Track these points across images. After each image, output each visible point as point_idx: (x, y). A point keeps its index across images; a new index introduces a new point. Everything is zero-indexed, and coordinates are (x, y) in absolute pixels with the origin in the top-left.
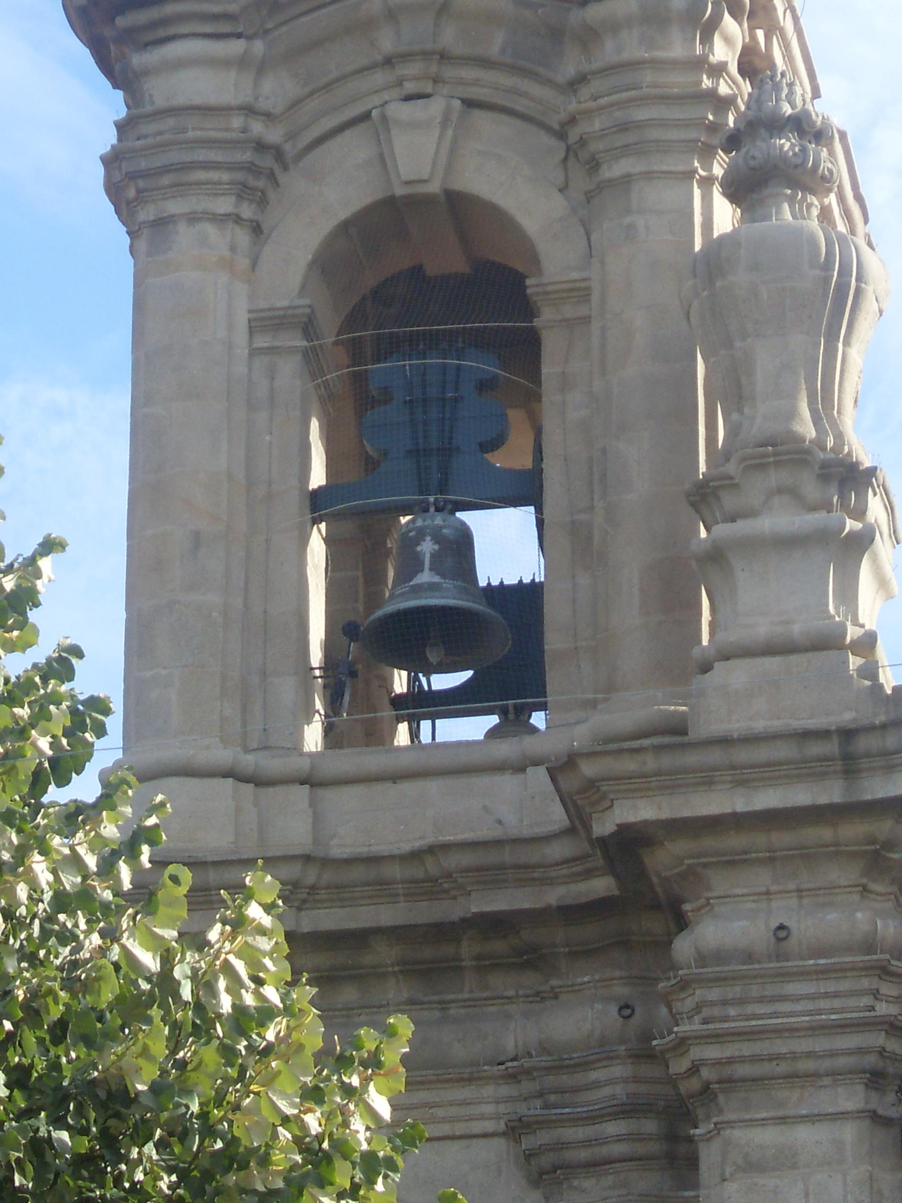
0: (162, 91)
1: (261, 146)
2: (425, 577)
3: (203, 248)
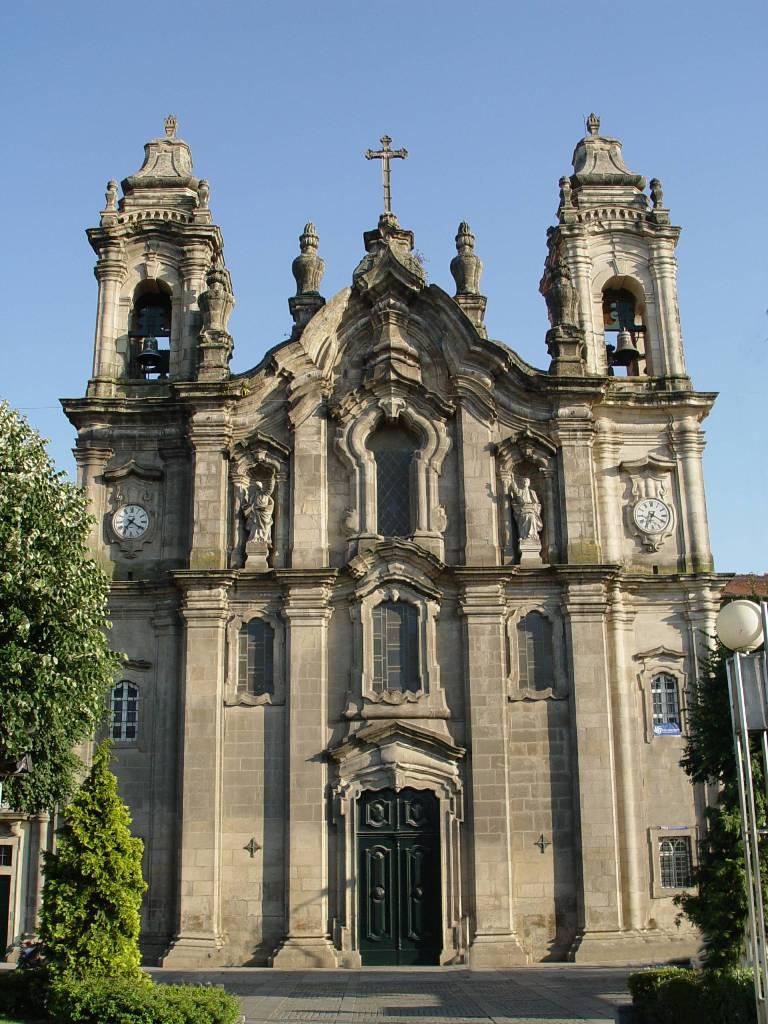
2: (149, 349)
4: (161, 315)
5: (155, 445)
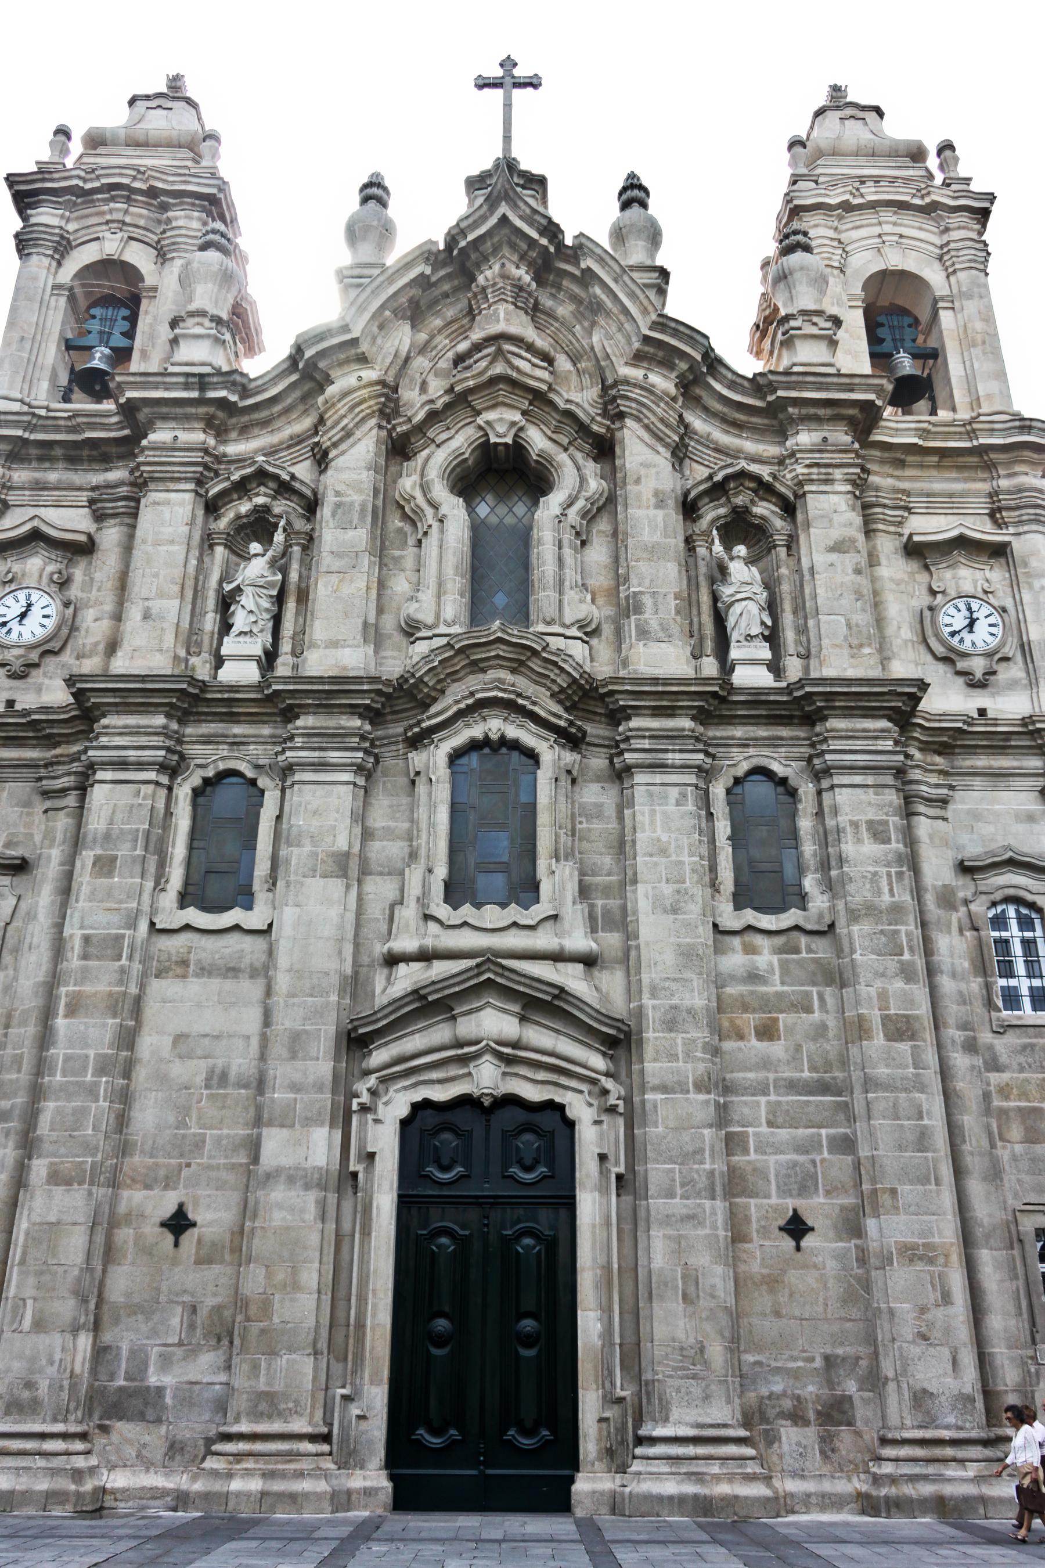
0: (33, 220)
1: (62, 237)
3: (40, 263)
4: (124, 318)
5: (84, 497)
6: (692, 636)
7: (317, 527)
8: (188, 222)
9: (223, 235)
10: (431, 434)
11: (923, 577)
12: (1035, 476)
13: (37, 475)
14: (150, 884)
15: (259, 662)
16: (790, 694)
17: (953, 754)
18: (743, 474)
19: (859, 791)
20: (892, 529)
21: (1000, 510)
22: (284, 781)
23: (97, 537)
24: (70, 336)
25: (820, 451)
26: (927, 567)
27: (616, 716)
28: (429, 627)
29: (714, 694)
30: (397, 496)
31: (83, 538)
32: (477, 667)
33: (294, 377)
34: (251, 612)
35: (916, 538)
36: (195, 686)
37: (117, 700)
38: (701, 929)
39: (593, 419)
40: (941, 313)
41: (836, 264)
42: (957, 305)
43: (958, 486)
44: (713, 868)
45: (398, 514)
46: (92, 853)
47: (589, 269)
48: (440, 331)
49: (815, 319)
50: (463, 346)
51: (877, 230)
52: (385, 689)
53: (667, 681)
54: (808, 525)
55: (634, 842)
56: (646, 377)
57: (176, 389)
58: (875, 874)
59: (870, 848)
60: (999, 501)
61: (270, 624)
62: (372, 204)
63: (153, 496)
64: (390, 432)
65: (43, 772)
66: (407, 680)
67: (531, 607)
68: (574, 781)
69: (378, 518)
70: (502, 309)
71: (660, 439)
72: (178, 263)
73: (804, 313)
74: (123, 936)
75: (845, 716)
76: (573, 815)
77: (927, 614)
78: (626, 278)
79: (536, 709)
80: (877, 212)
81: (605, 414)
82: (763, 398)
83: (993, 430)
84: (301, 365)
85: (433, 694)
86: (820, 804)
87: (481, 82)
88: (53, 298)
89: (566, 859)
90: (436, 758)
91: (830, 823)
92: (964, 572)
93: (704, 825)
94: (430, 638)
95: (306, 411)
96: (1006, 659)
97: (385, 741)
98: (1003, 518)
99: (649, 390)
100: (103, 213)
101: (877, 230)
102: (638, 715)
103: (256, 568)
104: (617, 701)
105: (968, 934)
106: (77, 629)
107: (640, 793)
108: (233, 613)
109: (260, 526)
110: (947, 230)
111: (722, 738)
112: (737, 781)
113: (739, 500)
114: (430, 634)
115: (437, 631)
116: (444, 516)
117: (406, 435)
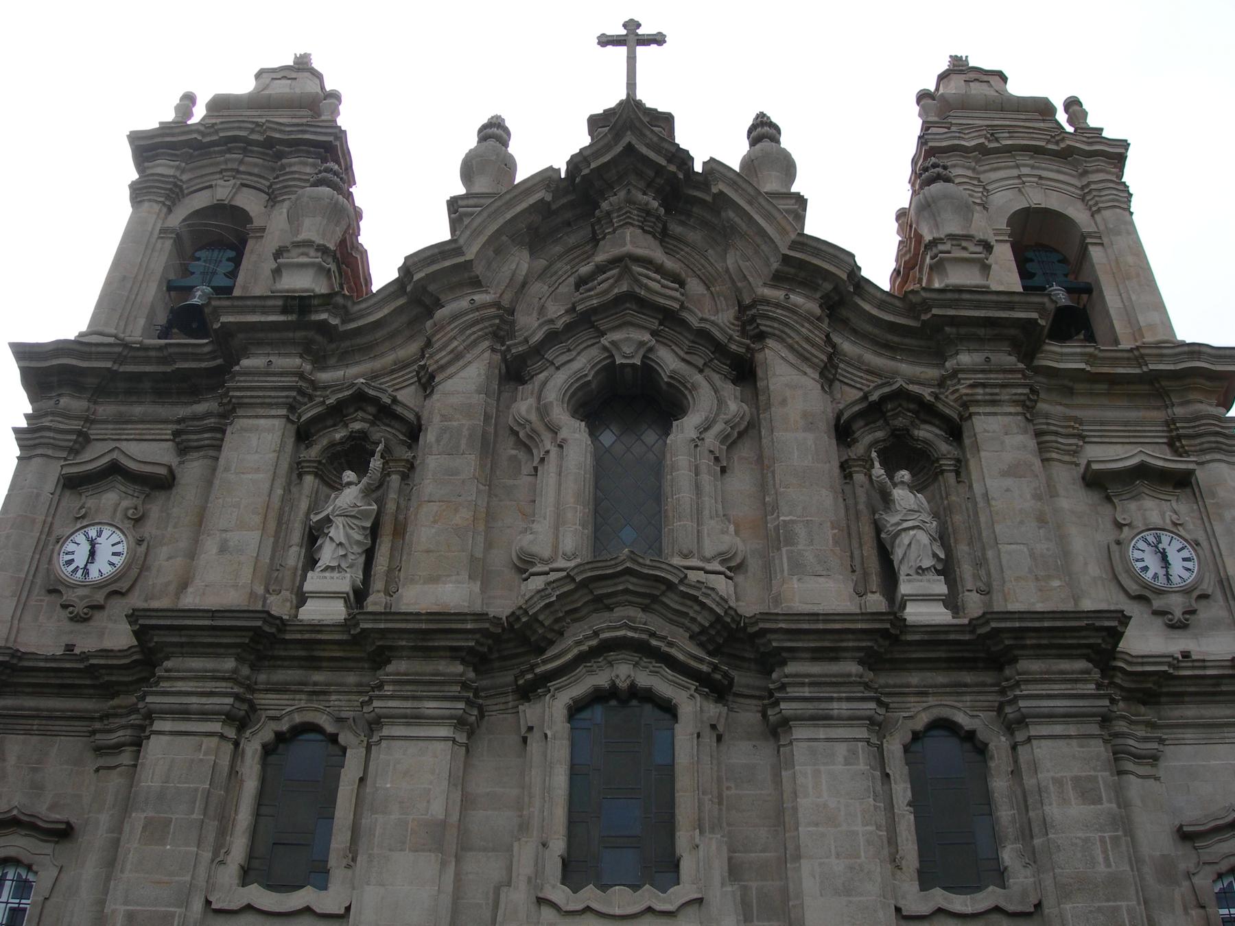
1: (175, 185)
3: (152, 209)
4: (229, 260)
6: (853, 571)
7: (420, 454)
8: (303, 166)
9: (335, 173)
10: (549, 355)
11: (1106, 509)
12: (1211, 405)
13: (123, 408)
14: (207, 855)
15: (346, 600)
16: (972, 632)
17: (1158, 703)
18: (901, 394)
19: (1061, 743)
20: (1067, 458)
21: (1179, 438)
22: (370, 737)
23: (177, 472)
24: (172, 277)
25: (983, 371)
26: (1109, 499)
27: (769, 661)
28: (544, 561)
29: (884, 633)
30: (511, 422)
31: (163, 471)
32: (602, 604)
33: (401, 301)
34: (340, 544)
35: (1095, 466)
36: (271, 625)
37: (183, 640)
38: (881, 914)
39: (731, 338)
40: (1091, 248)
41: (978, 201)
42: (1105, 240)
43: (1133, 415)
44: (892, 841)
45: (512, 439)
46: (143, 816)
47: (721, 192)
48: (560, 257)
49: (964, 244)
50: (585, 269)
51: (1015, 172)
52: (492, 629)
53: (828, 617)
54: (977, 449)
55: (795, 810)
56: (787, 297)
57: (273, 313)
58: (1086, 840)
59: (1077, 810)
60: (1177, 429)
61: (362, 559)
62: (491, 142)
63: (241, 423)
64: (504, 359)
65: (97, 725)
66: (518, 619)
67: (665, 541)
68: (719, 738)
69: (487, 447)
70: (628, 232)
71: (805, 359)
72: (287, 204)
73: (952, 237)
74: (173, 915)
75: (1038, 657)
76: (719, 780)
77: (1114, 547)
78: (761, 200)
79: (673, 651)
80: (1014, 156)
81: (743, 333)
82: (917, 318)
83: (1162, 355)
84: (409, 289)
85: (549, 636)
86: (1016, 761)
87: (604, 39)
88: (160, 241)
89: (712, 831)
90: (552, 711)
91: (1029, 782)
92: (1149, 503)
93: (879, 787)
94: (547, 573)
95: (412, 336)
96: (1204, 597)
97: (492, 692)
98: (1183, 447)
99: (793, 311)
100: (218, 164)
101: (1015, 172)
102: (794, 659)
103: (349, 497)
104: (770, 641)
105: (1193, 913)
106: (148, 569)
107: (800, 750)
108: (321, 546)
109: (355, 454)
110: (1085, 173)
111: (895, 686)
112: (916, 736)
113: (900, 422)
114: (546, 569)
115: (555, 565)
116: (564, 440)
117: (522, 359)
